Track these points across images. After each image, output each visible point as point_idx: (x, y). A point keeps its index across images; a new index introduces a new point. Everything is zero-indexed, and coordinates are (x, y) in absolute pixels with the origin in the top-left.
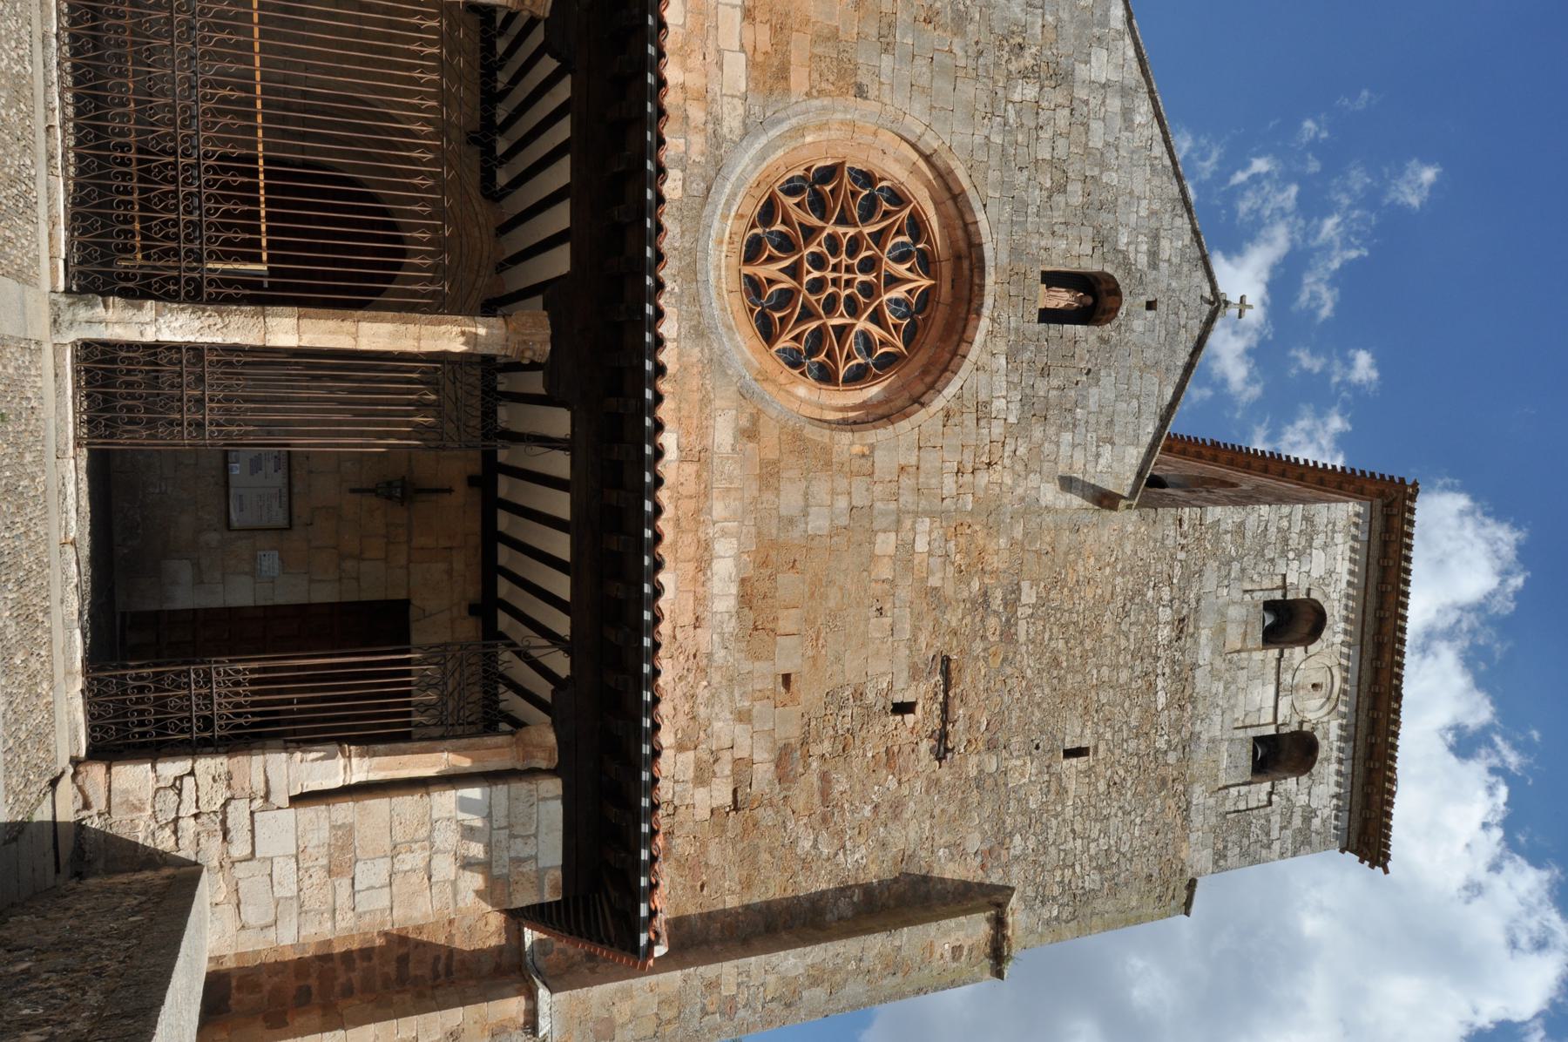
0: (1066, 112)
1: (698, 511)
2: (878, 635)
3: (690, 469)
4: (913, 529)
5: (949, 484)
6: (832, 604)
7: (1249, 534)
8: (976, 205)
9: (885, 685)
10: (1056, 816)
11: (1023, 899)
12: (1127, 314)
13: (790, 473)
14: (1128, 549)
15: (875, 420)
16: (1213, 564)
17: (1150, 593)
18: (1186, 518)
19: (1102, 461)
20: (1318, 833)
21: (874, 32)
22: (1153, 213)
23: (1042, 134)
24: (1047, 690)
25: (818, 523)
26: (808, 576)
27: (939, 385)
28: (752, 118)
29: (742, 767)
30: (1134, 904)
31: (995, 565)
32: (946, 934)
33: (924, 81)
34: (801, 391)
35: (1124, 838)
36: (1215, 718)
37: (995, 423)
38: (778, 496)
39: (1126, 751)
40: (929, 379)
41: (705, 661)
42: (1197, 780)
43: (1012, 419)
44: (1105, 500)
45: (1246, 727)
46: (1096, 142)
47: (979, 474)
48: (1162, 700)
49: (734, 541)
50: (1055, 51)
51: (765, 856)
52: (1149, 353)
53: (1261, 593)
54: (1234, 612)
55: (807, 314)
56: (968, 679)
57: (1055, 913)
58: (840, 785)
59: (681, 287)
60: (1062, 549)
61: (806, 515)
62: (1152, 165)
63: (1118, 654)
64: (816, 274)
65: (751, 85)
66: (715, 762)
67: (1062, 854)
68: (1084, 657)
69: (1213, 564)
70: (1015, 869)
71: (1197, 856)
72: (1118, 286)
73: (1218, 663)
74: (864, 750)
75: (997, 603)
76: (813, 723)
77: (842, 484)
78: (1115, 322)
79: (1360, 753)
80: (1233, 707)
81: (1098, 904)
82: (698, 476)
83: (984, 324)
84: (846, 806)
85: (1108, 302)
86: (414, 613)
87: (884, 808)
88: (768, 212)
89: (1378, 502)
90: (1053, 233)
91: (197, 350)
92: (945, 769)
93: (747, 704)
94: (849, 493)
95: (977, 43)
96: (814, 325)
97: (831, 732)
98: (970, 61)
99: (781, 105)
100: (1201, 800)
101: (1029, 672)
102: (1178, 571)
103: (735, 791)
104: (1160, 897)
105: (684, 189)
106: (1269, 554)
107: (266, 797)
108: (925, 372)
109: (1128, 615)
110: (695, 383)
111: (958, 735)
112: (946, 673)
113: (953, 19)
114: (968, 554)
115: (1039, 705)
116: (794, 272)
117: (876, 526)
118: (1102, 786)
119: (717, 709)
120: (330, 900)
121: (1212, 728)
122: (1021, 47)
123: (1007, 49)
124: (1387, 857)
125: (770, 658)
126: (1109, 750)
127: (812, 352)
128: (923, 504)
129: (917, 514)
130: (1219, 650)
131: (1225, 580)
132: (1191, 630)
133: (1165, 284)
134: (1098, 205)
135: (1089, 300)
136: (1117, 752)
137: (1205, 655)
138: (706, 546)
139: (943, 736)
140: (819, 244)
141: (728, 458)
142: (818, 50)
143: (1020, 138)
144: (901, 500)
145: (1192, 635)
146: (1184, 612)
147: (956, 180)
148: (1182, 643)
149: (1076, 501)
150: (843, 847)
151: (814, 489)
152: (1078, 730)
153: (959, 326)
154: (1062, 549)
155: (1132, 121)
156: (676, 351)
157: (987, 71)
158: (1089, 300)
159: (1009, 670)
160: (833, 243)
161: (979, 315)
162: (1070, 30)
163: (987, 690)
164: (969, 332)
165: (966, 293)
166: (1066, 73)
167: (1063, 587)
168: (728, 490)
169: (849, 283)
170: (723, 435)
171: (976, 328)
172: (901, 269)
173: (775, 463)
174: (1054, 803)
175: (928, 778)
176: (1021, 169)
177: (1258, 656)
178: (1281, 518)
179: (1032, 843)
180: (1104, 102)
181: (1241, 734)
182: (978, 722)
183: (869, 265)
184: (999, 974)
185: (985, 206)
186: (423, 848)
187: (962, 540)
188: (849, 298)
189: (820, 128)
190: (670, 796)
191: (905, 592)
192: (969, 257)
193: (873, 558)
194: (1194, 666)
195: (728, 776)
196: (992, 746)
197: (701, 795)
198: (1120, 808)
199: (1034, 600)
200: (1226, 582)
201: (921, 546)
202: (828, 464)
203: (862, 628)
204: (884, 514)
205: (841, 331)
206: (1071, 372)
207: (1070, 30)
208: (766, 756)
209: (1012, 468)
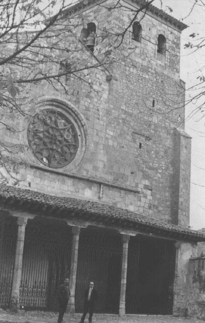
4: (109, 135)
5: (101, 122)
8: (43, 98)
17: (127, 73)
18: (113, 57)
19: (100, 78)
25: (105, 159)
29: (146, 187)
40: (78, 121)
43: (89, 101)
48: (147, 77)
61: (103, 161)
73: (142, 57)
75: (124, 116)
79: (165, 22)
103: (149, 190)
111: (147, 133)
115: (144, 111)
125: (128, 176)
128: (104, 131)
129: (106, 133)
153: (67, 109)
164: (70, 107)
171: (70, 106)
173: (94, 167)
179: (167, 120)
184: (191, 138)
187: (112, 122)
192: (53, 101)
193: (113, 146)
196: (150, 125)
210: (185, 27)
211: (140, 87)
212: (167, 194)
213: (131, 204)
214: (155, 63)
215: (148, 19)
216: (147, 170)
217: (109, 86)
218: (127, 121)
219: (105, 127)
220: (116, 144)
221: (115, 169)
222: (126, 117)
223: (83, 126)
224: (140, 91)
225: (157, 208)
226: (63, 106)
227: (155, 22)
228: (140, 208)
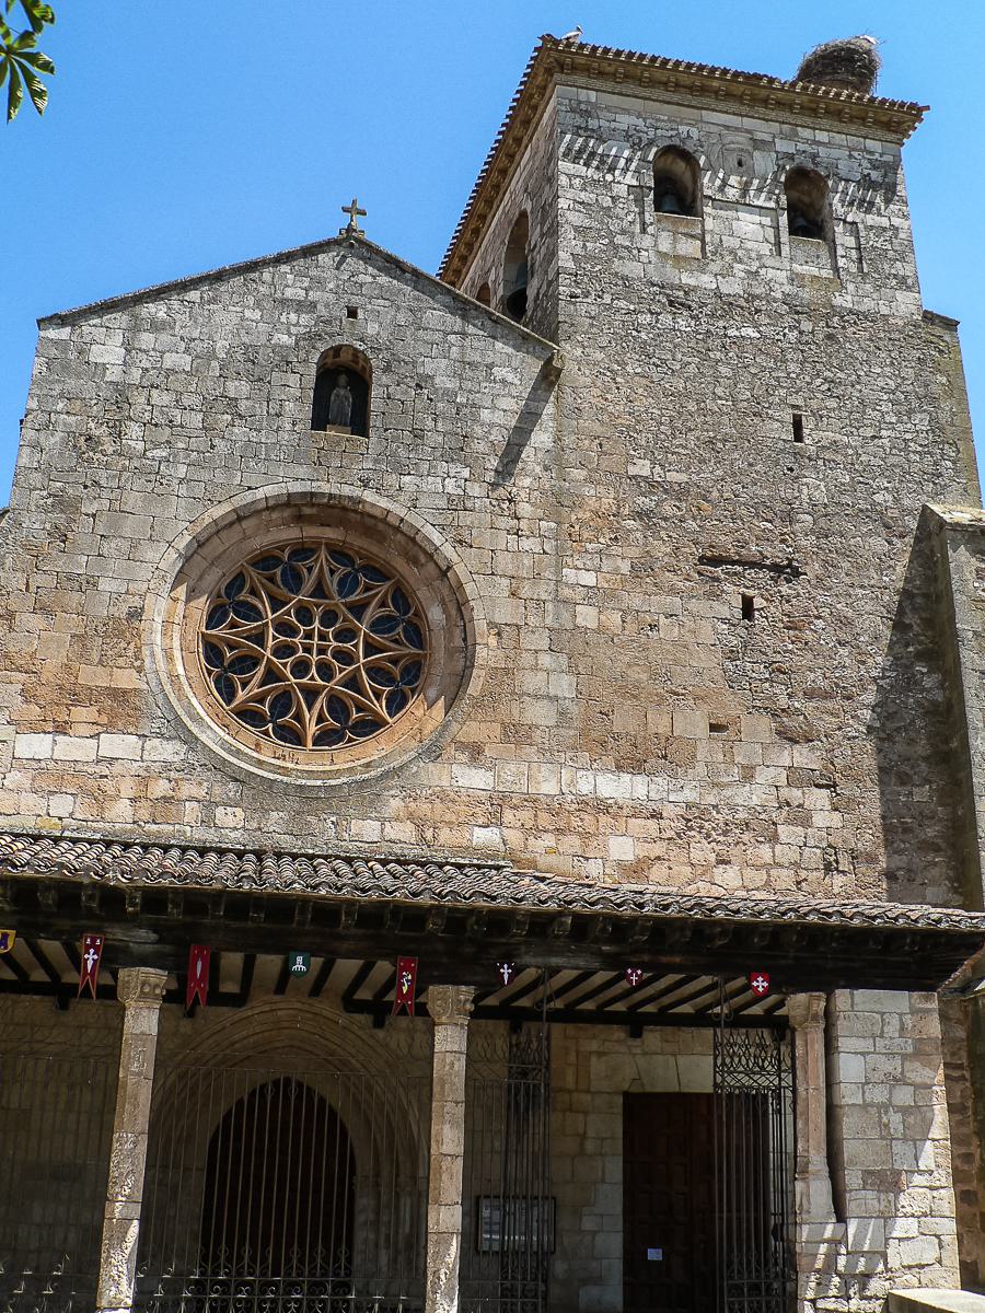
0: (155, 393)
1: (549, 810)
2: (676, 630)
3: (508, 815)
4: (572, 586)
5: (526, 544)
7: (587, 223)
8: (249, 497)
9: (725, 626)
11: (935, 496)
13: (516, 712)
14: (599, 356)
15: (463, 619)
16: (617, 265)
19: (510, 377)
20: (885, 176)
21: (76, 596)
22: (258, 304)
23: (178, 421)
25: (564, 686)
27: (430, 549)
28: (164, 730)
29: (796, 777)
30: (944, 380)
31: (611, 501)
33: (125, 545)
35: (882, 384)
36: (770, 276)
39: (798, 375)
40: (423, 559)
42: (829, 300)
43: (466, 473)
44: (549, 377)
45: (778, 244)
46: (185, 361)
48: (751, 332)
50: (94, 401)
53: (647, 215)
54: (665, 246)
55: (353, 682)
56: (723, 538)
57: (949, 464)
58: (815, 679)
60: (598, 428)
61: (556, 698)
62: (209, 302)
64: (314, 670)
65: (131, 730)
66: (788, 804)
67: (894, 451)
68: (703, 412)
69: (617, 265)
70: (906, 502)
71: (905, 305)
72: (332, 347)
73: (715, 267)
74: (785, 652)
75: (645, 502)
77: (527, 659)
78: (369, 354)
79: (809, 121)
80: (759, 257)
81: (944, 417)
82: (515, 807)
83: (369, 496)
85: (345, 357)
86: (635, 1089)
87: (842, 636)
88: (248, 716)
90: (278, 415)
92: (807, 569)
95: (86, 487)
97: (767, 685)
98: (105, 494)
99: (151, 699)
100: (849, 298)
102: (623, 304)
103: (818, 786)
104: (941, 352)
106: (607, 202)
108: (415, 561)
109: (664, 361)
111: (775, 553)
112: (716, 561)
113: (62, 511)
114: (599, 530)
116: (311, 694)
117: (569, 626)
118: (832, 403)
120: (921, 1190)
121: (778, 277)
122: (89, 439)
123: (91, 454)
124: (913, 106)
126: (797, 393)
130: (701, 263)
131: (633, 252)
132: (681, 294)
133: (331, 296)
134: (255, 364)
135: (343, 379)
137: (707, 281)
138: (583, 804)
139: (776, 568)
140: (285, 665)
141: (499, 776)
142: (95, 657)
143: (181, 445)
148: (694, 305)
149: (549, 409)
152: (776, 425)
155: (163, 322)
157: (115, 476)
158: (343, 379)
159: (715, 494)
160: (283, 651)
161: (360, 501)
162: (72, 384)
164: (377, 513)
166: (117, 390)
169: (323, 637)
170: (477, 779)
172: (309, 583)
174: (846, 456)
175: (815, 588)
176: (213, 447)
177: (709, 224)
178: (571, 186)
180: (145, 351)
181: (785, 249)
182: (764, 531)
183: (304, 615)
185: (250, 488)
186: (886, 1112)
187: (586, 535)
188: (338, 636)
189: (170, 658)
190: (818, 851)
191: (636, 601)
192: (298, 508)
194: (718, 294)
195: (803, 793)
196: (789, 517)
197: (820, 820)
198: (853, 386)
200: (635, 252)
201: (589, 579)
203: (668, 647)
204: (557, 617)
205: (371, 648)
206: (419, 406)
207: (72, 384)
208: (786, 752)
210: (915, 112)
212: (922, 794)
213: (723, 862)
214: (782, 276)
215: (727, 127)
218: (665, 519)
220: (617, 617)
225: (871, 859)
227: (763, 130)
228: (774, 872)
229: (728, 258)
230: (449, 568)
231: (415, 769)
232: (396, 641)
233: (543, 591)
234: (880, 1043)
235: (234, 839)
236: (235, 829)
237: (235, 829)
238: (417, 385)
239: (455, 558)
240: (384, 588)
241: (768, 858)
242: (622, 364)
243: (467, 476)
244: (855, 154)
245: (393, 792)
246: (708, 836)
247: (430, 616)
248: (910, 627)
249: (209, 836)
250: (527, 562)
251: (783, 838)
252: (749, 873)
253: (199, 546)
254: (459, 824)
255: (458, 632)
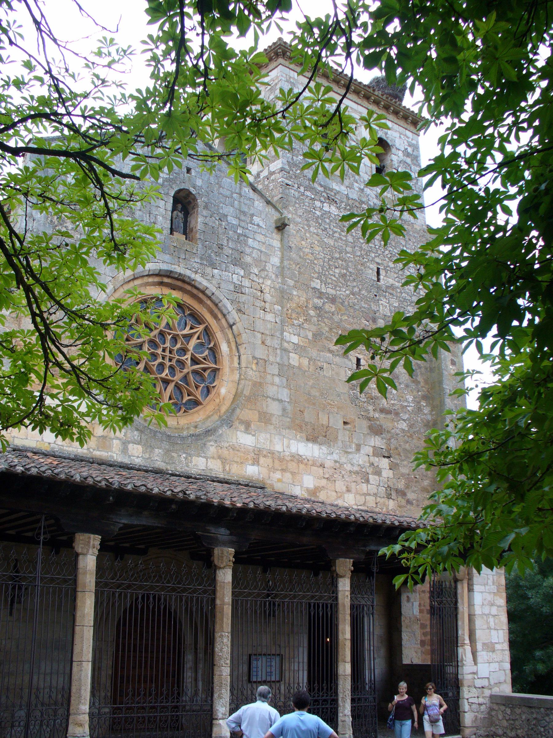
3: (262, 460)
4: (288, 342)
5: (270, 317)
6: (317, 394)
10: (402, 293)
12: (194, 188)
13: (264, 406)
17: (318, 213)
19: (261, 224)
24: (355, 284)
25: (284, 394)
26: (307, 405)
27: (225, 312)
29: (377, 452)
32: (447, 367)
34: (223, 391)
36: (368, 193)
37: (243, 284)
38: (274, 415)
40: (220, 316)
41: (337, 464)
43: (242, 273)
47: (266, 299)
49: (292, 441)
51: (407, 446)
52: (212, 180)
59: (185, 453)
61: (280, 401)
63: (342, 239)
64: (167, 371)
66: (373, 464)
73: (346, 182)
76: (362, 413)
77: (269, 377)
78: (197, 196)
82: (265, 456)
83: (198, 278)
84: (392, 402)
89: (281, 60)
90: (155, 223)
91: (353, 700)
93: (354, 446)
94: (273, 375)
96: (191, 377)
97: (366, 404)
101: (348, 292)
102: (308, 193)
103: (384, 457)
105: (138, 444)
107: (474, 673)
108: (215, 317)
109: (326, 229)
110: (225, 453)
116: (166, 382)
117: (286, 363)
119: (355, 462)
127: (203, 380)
128: (278, 334)
129: (282, 339)
132: (333, 194)
136: (379, 252)
137: (343, 189)
138: (293, 456)
144: (276, 346)
145: (335, 194)
146: (325, 195)
147: (128, 277)
150: (406, 406)
151: (271, 394)
153: (195, 291)
154: (300, 260)
156: (212, 460)
159: (346, 303)
163: (353, 318)
164: (201, 287)
165: (179, 283)
167: (314, 263)
168: (271, 441)
169: (170, 352)
174: (396, 292)
187: (294, 316)
193: (299, 368)
199: (319, 281)
201: (295, 339)
202: (260, 384)
203: (327, 380)
204: (282, 358)
205: (195, 361)
208: (373, 439)
209: (264, 278)
211: (346, 241)
213: (348, 490)
216: (377, 415)
217: (282, 240)
218: (326, 312)
219: (278, 326)
220: (305, 362)
221: (308, 416)
222: (324, 304)
223: (231, 326)
224: (349, 249)
225: (403, 494)
226: (189, 288)
228: (367, 497)
229: (352, 179)
230: (234, 324)
231: (221, 432)
232: (204, 359)
233: (276, 343)
234: (487, 587)
235: (138, 461)
236: (138, 457)
237: (138, 457)
238: (220, 219)
239: (238, 320)
240: (201, 327)
241: (365, 491)
242: (309, 226)
243: (243, 274)
244: (402, 136)
245: (211, 443)
246: (343, 477)
247: (222, 348)
248: (419, 382)
249: (126, 460)
250: (269, 326)
251: (371, 482)
252: (358, 496)
253: (115, 291)
254: (242, 463)
255: (236, 359)
